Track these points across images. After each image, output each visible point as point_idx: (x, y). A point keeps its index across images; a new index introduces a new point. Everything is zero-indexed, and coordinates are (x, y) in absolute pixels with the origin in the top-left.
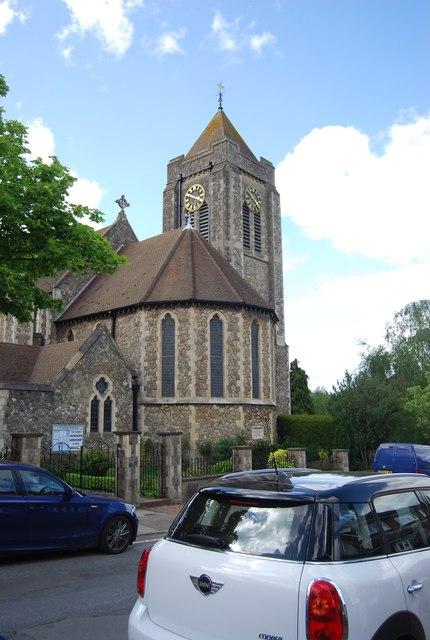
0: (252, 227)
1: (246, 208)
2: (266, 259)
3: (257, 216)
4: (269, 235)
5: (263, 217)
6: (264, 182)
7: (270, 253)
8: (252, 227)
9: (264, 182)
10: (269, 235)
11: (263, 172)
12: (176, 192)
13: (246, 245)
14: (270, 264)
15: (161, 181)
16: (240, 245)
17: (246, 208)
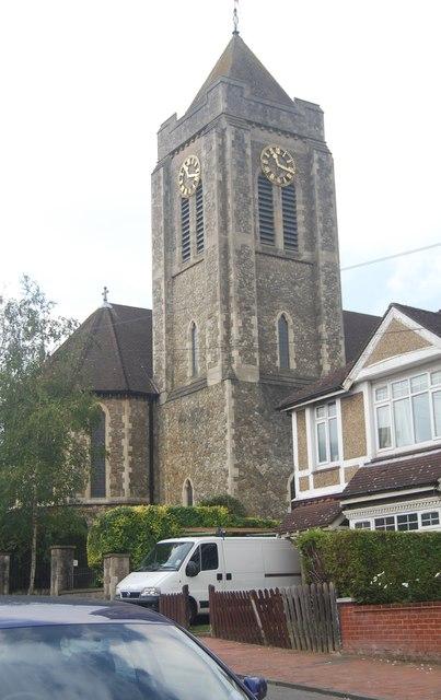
0: (278, 216)
1: (264, 182)
2: (306, 256)
3: (288, 193)
4: (311, 214)
5: (299, 195)
6: (301, 137)
7: (311, 246)
8: (278, 216)
9: (301, 137)
10: (311, 214)
11: (304, 123)
12: (167, 170)
13: (267, 234)
14: (313, 264)
15: (151, 158)
16: (251, 242)
17: (264, 182)
